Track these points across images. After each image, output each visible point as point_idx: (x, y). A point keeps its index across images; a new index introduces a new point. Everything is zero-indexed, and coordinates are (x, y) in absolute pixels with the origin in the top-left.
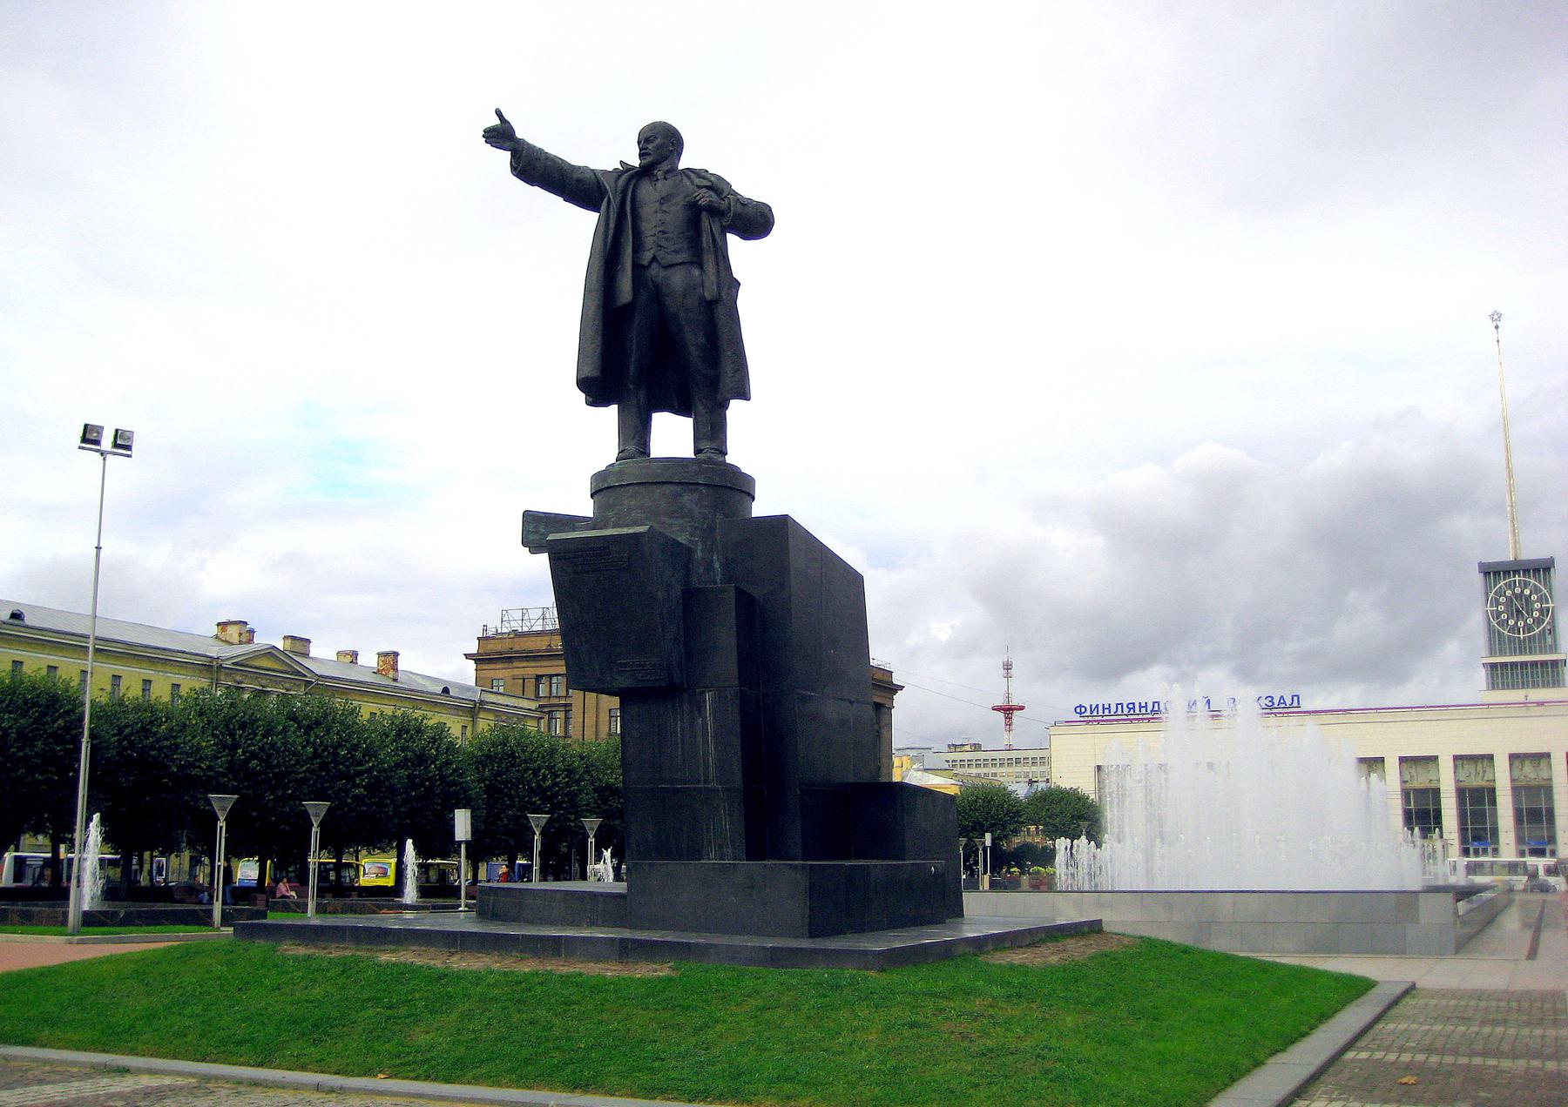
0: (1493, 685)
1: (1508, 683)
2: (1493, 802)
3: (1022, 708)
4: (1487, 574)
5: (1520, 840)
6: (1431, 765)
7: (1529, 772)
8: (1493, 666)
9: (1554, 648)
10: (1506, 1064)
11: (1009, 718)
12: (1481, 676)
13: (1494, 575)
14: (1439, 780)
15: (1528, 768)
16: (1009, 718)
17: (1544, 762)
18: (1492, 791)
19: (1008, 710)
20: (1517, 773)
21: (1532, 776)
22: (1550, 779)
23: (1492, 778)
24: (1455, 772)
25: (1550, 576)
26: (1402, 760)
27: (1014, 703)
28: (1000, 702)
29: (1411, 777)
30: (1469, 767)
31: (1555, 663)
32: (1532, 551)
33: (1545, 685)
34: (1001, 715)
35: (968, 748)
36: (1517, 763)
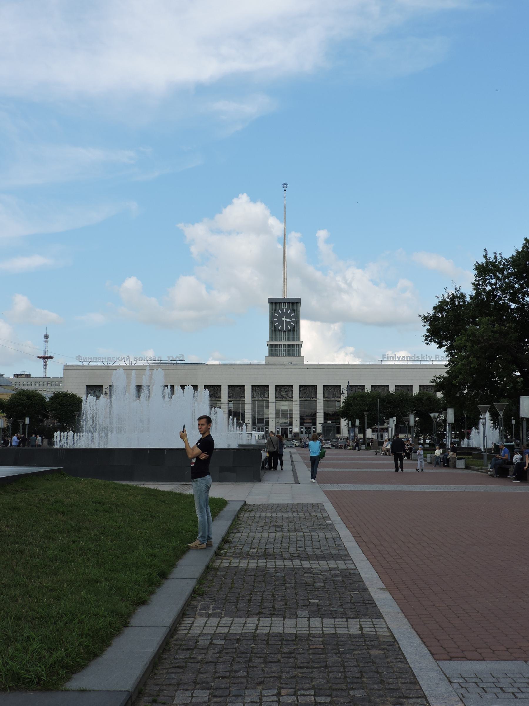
0: (271, 354)
1: (273, 353)
2: (268, 407)
3: (52, 358)
4: (271, 303)
8: (272, 345)
9: (298, 338)
10: (314, 565)
11: (45, 362)
12: (266, 350)
13: (275, 304)
16: (45, 362)
19: (45, 358)
20: (278, 393)
24: (252, 393)
25: (298, 305)
27: (49, 355)
28: (42, 354)
31: (297, 345)
32: (290, 295)
33: (293, 355)
34: (42, 361)
35: (24, 376)
36: (278, 388)
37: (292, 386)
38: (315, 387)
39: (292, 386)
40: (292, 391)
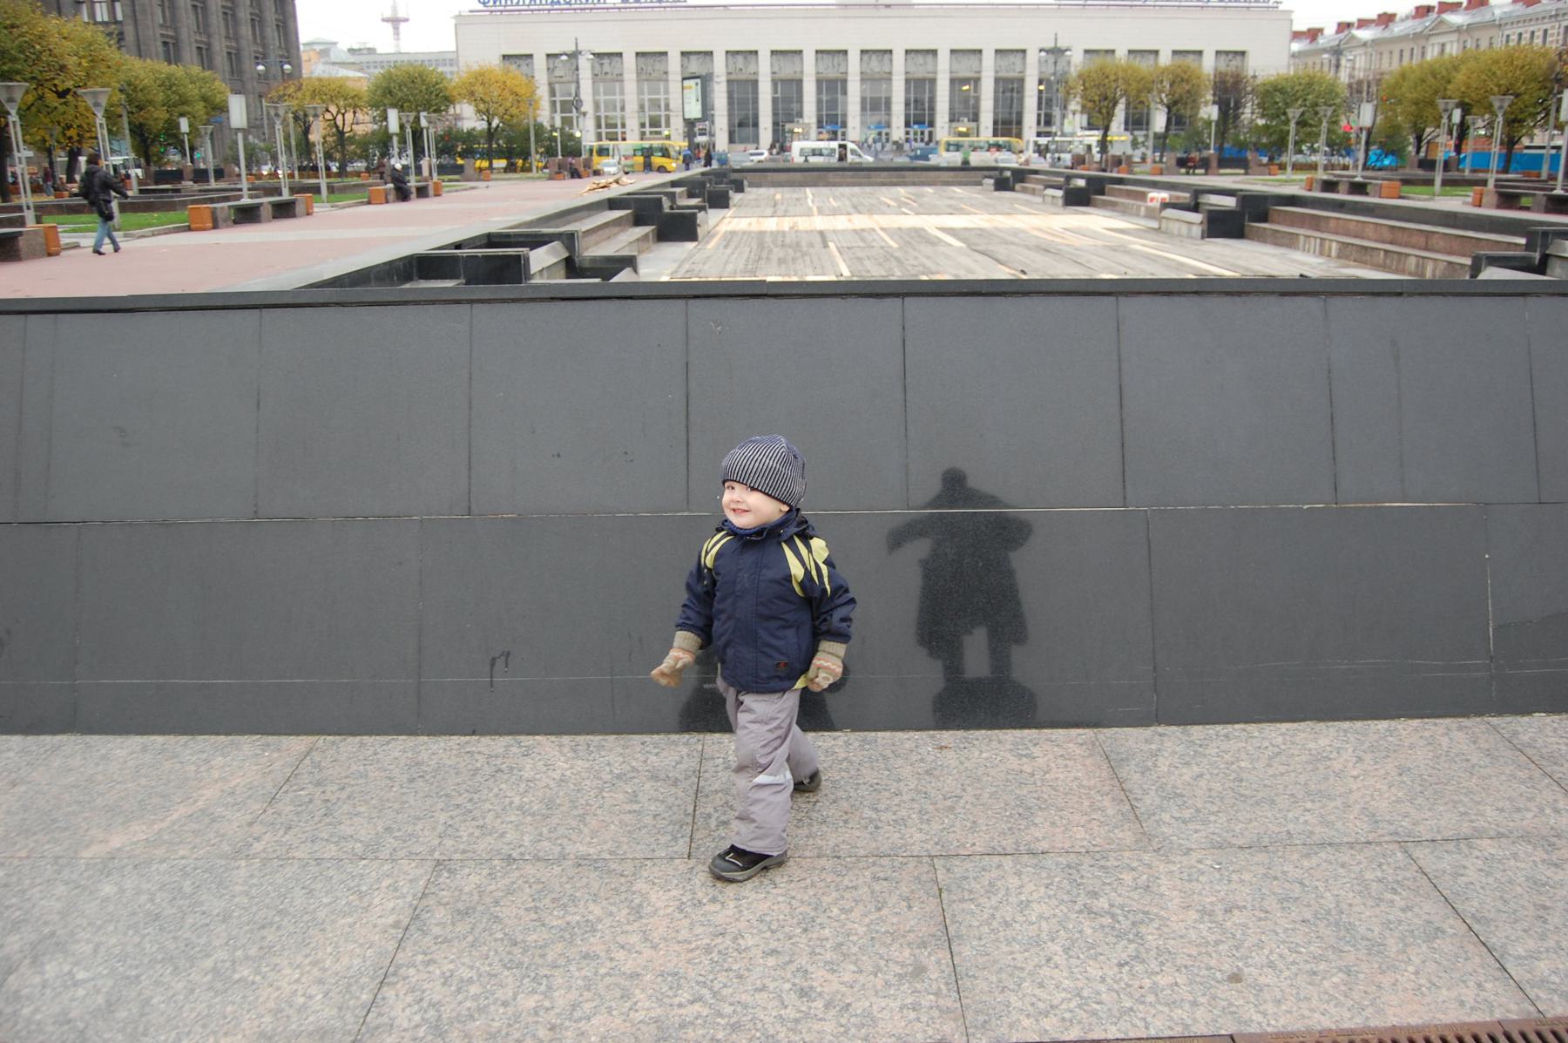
2: (845, 93)
5: (863, 123)
6: (796, 58)
7: (875, 65)
14: (802, 72)
15: (875, 65)
17: (887, 56)
18: (844, 82)
21: (877, 70)
22: (890, 73)
23: (843, 70)
26: (773, 52)
29: (780, 68)
30: (827, 59)
36: (866, 57)
37: (891, 51)
38: (934, 52)
39: (891, 51)
40: (891, 60)
